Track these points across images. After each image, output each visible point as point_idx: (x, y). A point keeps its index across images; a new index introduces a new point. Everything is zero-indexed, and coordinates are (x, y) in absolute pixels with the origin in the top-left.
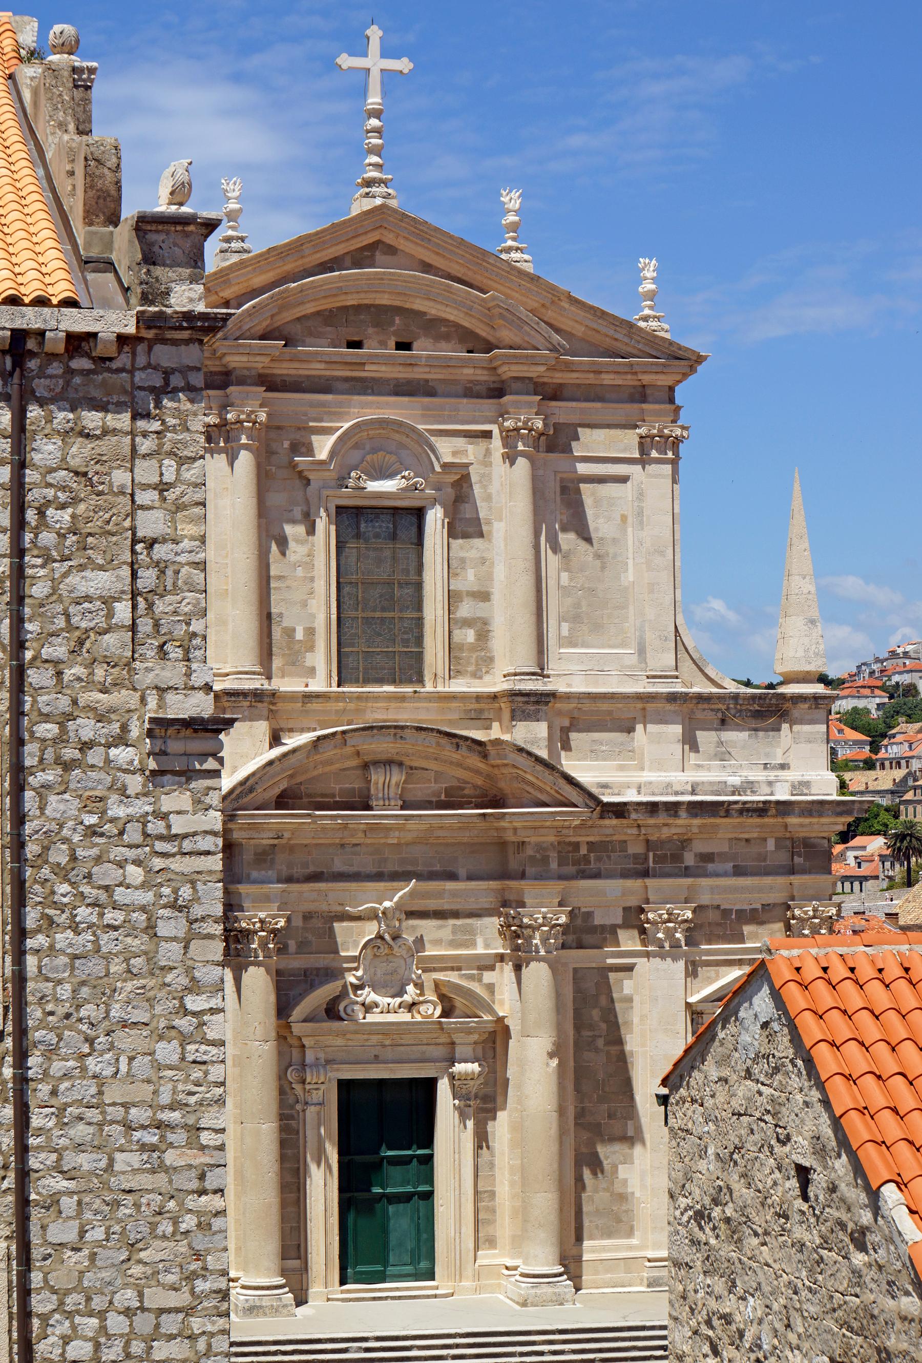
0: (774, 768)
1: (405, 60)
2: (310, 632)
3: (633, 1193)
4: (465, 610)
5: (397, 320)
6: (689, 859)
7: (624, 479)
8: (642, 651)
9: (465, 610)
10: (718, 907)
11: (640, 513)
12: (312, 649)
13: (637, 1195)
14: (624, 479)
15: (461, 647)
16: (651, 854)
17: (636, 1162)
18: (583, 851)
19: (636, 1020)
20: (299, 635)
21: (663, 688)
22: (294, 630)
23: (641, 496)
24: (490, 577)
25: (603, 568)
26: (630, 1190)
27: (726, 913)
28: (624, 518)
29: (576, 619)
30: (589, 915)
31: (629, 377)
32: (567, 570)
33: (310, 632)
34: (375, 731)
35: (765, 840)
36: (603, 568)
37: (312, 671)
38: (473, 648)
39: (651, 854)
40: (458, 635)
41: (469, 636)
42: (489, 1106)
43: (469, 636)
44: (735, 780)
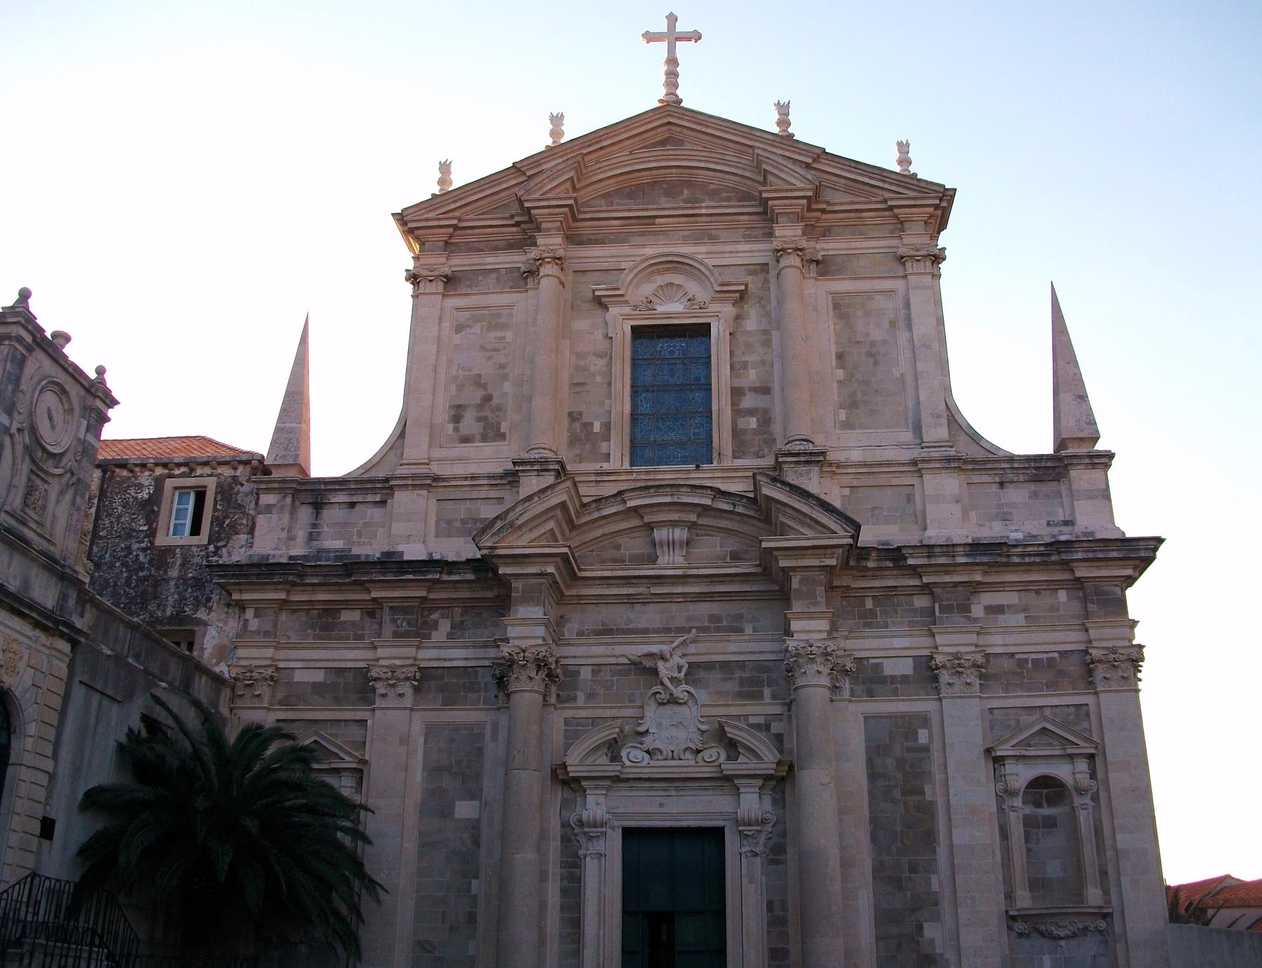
0: (1057, 525)
2: (607, 426)
4: (748, 401)
5: (685, 192)
6: (977, 611)
9: (748, 401)
10: (1012, 655)
16: (937, 605)
18: (869, 604)
20: (597, 427)
22: (592, 424)
23: (907, 305)
24: (770, 374)
25: (876, 363)
27: (1022, 663)
30: (878, 667)
32: (843, 368)
33: (607, 426)
36: (876, 363)
37: (607, 457)
38: (755, 432)
39: (937, 605)
41: (753, 423)
42: (780, 858)
43: (753, 423)
44: (1019, 536)
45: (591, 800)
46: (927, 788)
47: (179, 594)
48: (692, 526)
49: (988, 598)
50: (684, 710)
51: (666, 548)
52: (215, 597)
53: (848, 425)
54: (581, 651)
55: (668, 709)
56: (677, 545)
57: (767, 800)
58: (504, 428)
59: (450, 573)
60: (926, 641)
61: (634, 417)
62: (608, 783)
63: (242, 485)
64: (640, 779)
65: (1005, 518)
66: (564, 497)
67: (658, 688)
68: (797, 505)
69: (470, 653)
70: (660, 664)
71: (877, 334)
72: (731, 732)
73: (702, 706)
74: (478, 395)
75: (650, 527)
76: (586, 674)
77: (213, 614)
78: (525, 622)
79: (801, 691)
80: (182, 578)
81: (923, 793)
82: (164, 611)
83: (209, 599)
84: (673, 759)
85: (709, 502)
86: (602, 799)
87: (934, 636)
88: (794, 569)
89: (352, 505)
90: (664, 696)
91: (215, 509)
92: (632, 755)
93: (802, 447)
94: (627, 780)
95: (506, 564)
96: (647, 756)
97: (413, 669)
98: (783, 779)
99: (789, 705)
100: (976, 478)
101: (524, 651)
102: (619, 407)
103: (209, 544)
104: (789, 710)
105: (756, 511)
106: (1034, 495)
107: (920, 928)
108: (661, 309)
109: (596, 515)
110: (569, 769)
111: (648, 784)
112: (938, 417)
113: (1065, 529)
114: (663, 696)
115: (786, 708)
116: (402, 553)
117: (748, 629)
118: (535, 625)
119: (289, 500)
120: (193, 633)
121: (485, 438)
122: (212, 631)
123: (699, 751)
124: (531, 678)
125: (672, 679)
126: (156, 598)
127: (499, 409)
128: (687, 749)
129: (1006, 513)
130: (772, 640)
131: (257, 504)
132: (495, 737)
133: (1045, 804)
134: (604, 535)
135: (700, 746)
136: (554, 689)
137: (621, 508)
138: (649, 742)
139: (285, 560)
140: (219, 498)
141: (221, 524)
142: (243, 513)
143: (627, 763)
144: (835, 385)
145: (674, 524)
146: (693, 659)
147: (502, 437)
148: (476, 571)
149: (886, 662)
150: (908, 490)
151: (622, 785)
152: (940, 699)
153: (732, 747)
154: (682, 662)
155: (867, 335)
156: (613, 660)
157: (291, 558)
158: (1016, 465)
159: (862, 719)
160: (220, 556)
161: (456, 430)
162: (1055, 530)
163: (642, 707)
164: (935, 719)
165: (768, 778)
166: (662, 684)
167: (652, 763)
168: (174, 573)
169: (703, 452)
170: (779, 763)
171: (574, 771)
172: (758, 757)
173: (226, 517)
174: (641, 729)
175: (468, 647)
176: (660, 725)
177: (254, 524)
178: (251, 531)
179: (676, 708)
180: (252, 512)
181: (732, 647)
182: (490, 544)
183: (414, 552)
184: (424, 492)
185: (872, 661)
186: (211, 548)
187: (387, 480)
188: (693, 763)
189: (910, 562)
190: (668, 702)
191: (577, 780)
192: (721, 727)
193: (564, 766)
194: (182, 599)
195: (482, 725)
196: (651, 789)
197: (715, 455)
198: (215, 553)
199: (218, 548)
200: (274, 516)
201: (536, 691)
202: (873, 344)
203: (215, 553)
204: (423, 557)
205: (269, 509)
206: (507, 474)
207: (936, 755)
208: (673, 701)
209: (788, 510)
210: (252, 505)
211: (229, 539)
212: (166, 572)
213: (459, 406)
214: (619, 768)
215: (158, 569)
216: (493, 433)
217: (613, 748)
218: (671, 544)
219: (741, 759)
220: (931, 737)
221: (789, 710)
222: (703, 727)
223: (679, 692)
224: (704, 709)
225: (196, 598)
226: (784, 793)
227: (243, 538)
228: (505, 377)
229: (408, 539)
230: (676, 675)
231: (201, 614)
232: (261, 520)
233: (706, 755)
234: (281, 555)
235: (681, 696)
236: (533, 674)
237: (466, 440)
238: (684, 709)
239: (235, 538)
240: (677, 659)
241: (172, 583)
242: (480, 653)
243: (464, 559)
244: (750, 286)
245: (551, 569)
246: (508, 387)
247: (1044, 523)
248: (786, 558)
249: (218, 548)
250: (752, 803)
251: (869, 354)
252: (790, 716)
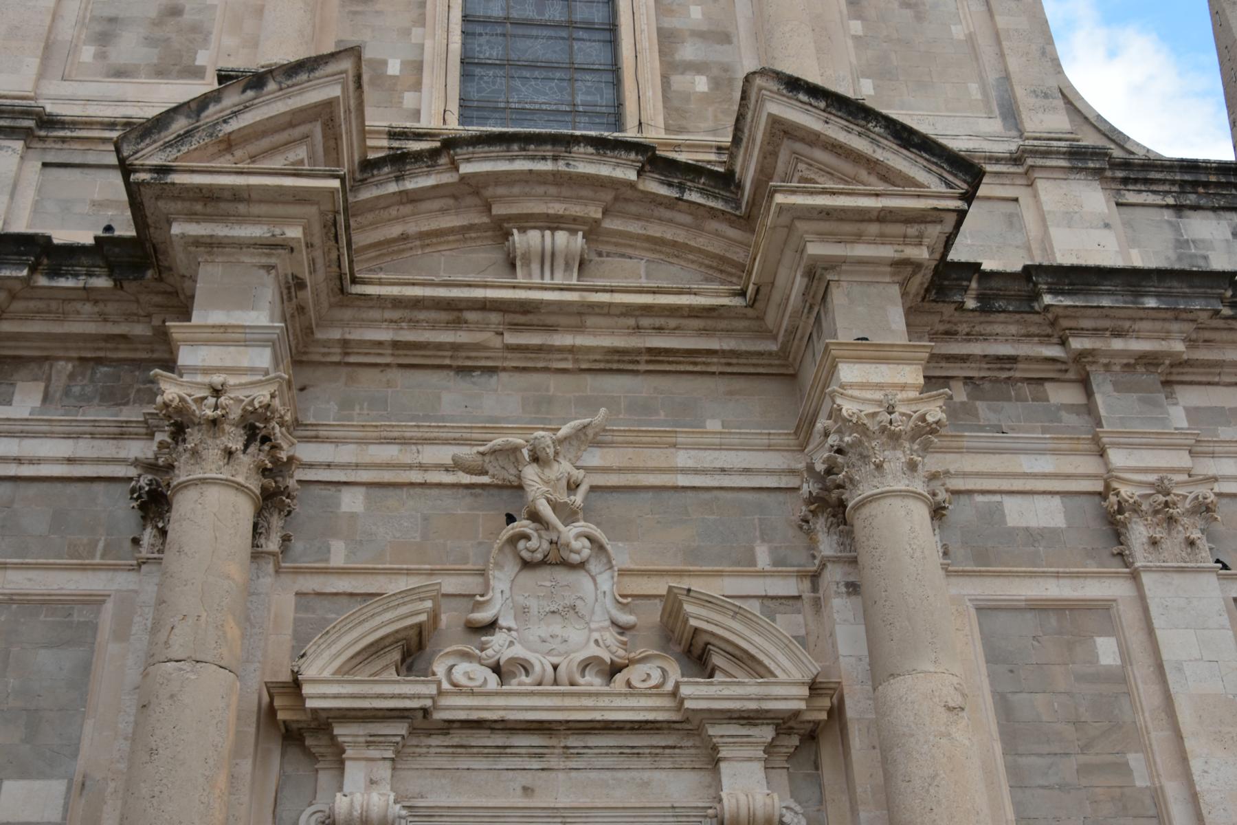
4: (688, 52)
9: (688, 52)
15: (687, 97)
20: (394, 68)
22: (384, 63)
32: (859, 17)
45: (355, 773)
46: (1135, 760)
48: (592, 231)
49: (1190, 397)
50: (582, 581)
51: (535, 267)
54: (346, 454)
55: (544, 577)
56: (560, 262)
57: (781, 777)
59: (54, 273)
60: (1089, 465)
61: (468, 63)
62: (401, 728)
64: (478, 724)
66: (335, 91)
67: (523, 525)
68: (842, 137)
69: (83, 448)
70: (531, 473)
72: (697, 616)
73: (623, 573)
75: (501, 230)
78: (223, 335)
79: (865, 511)
81: (1123, 768)
84: (556, 682)
85: (632, 175)
86: (384, 771)
87: (1102, 453)
88: (833, 264)
90: (537, 545)
92: (459, 680)
94: (449, 726)
95: (192, 217)
96: (493, 679)
98: (812, 736)
99: (815, 577)
100: (1131, 197)
101: (217, 392)
102: (440, 33)
104: (815, 588)
105: (726, 200)
109: (393, 188)
110: (307, 690)
111: (499, 739)
114: (534, 543)
115: (807, 584)
117: (713, 425)
118: (246, 343)
123: (613, 670)
124: (229, 454)
125: (555, 506)
127: (195, 28)
128: (585, 665)
130: (769, 448)
132: (122, 634)
134: (404, 237)
135: (621, 654)
136: (276, 521)
137: (448, 178)
138: (499, 646)
143: (446, 686)
144: (850, 43)
145: (553, 223)
146: (600, 480)
148: (112, 269)
149: (1010, 503)
150: (1010, 207)
151: (435, 741)
152: (1135, 576)
153: (697, 655)
154: (578, 475)
156: (416, 476)
158: (1203, 178)
159: (973, 612)
163: (482, 573)
164: (1128, 615)
165: (784, 723)
166: (535, 517)
170: (815, 688)
171: (322, 693)
174: (483, 616)
175: (77, 436)
176: (525, 610)
179: (563, 576)
181: (683, 459)
182: (156, 161)
184: (19, 145)
185: (979, 498)
189: (1048, 299)
190: (543, 563)
191: (323, 723)
192: (672, 605)
193: (295, 685)
195: (94, 601)
196: (502, 751)
201: (239, 487)
207: (1147, 694)
208: (557, 560)
209: (820, 155)
213: (112, 20)
214: (433, 690)
217: (412, 650)
218: (548, 259)
219: (719, 677)
220: (1124, 653)
221: (815, 588)
222: (626, 618)
223: (571, 534)
224: (626, 580)
226: (817, 768)
230: (563, 497)
233: (635, 674)
235: (576, 545)
236: (237, 444)
237: (120, 73)
238: (582, 579)
240: (563, 468)
242: (107, 449)
245: (294, 233)
248: (823, 237)
250: (747, 784)
252: (817, 604)
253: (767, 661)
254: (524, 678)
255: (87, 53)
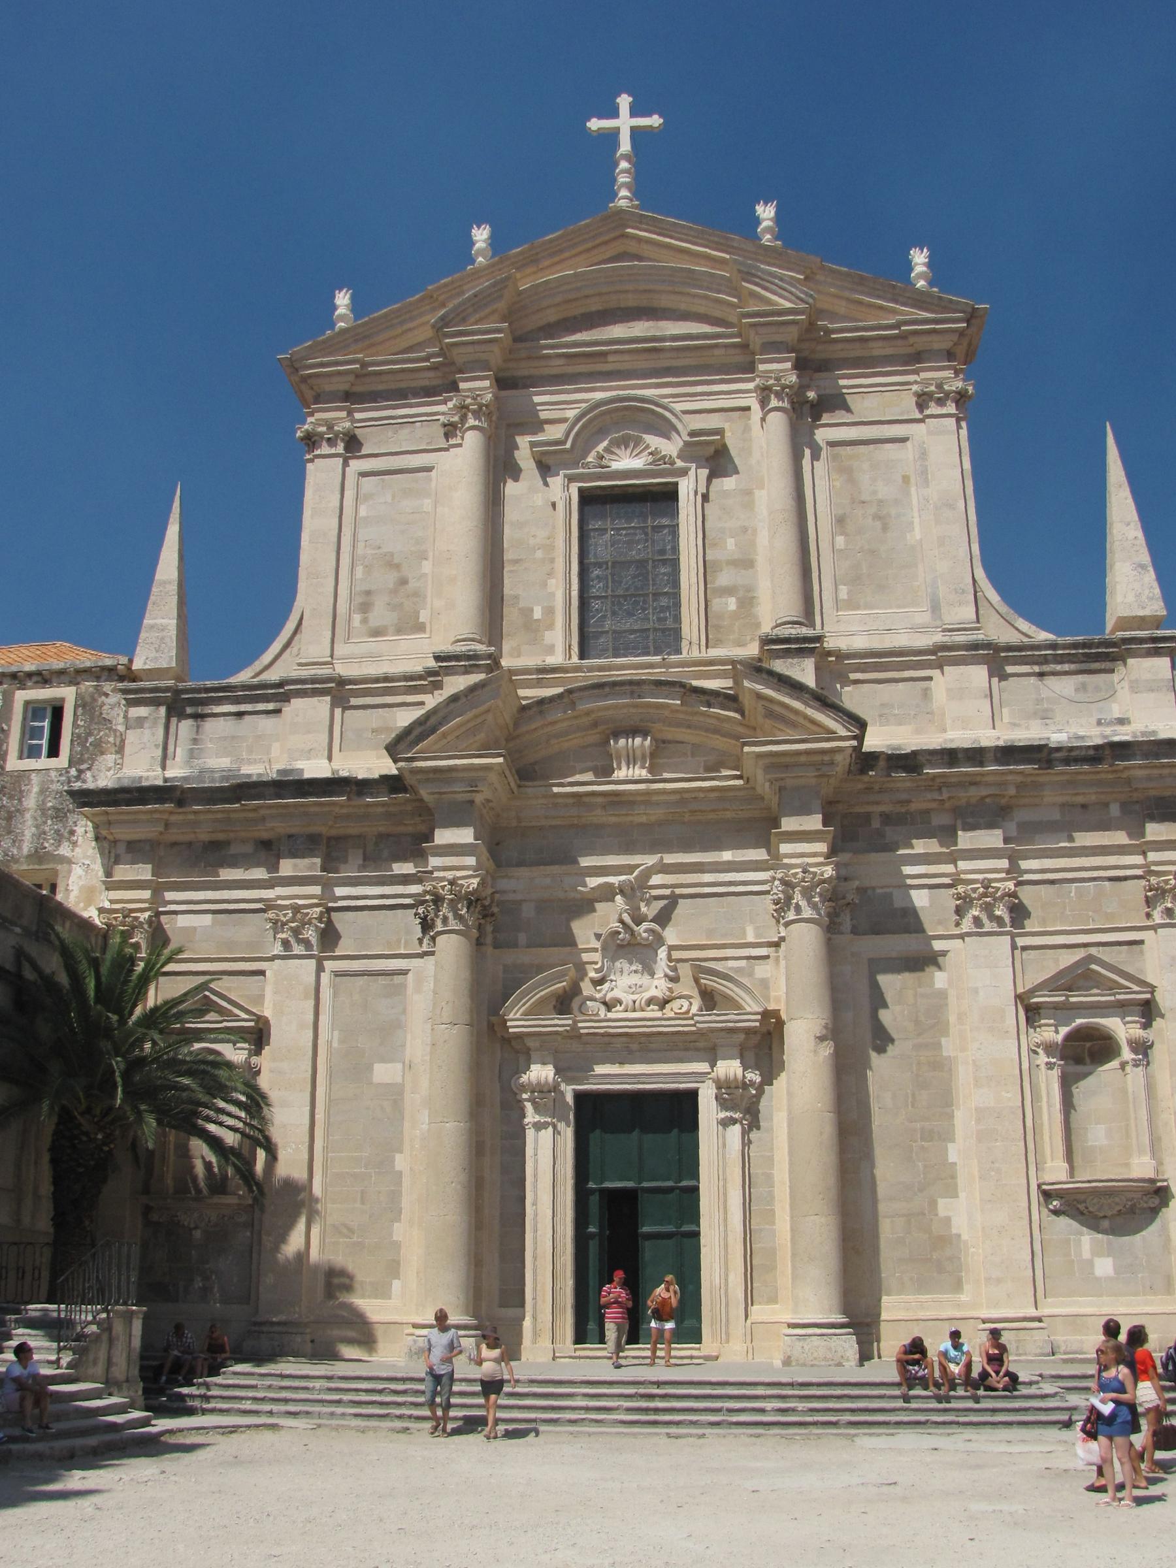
1: (656, 117)
3: (959, 1236)
4: (724, 579)
7: (904, 440)
8: (935, 608)
11: (924, 472)
12: (551, 626)
13: (965, 1237)
14: (904, 440)
17: (962, 1195)
18: (876, 824)
19: (952, 1019)
20: (538, 614)
21: (960, 638)
22: (532, 610)
23: (924, 454)
25: (885, 528)
26: (954, 1231)
28: (906, 479)
29: (855, 580)
31: (899, 342)
33: (549, 611)
34: (607, 690)
35: (1106, 805)
36: (885, 528)
38: (735, 616)
40: (716, 604)
43: (732, 604)
47: (37, 827)
52: (80, 830)
53: (852, 604)
58: (424, 616)
63: (107, 695)
65: (1045, 716)
71: (884, 491)
74: (391, 578)
76: (528, 911)
77: (77, 850)
80: (42, 809)
81: (938, 1046)
82: (20, 848)
83: (72, 833)
84: (634, 1010)
89: (240, 715)
91: (75, 725)
93: (793, 631)
97: (318, 910)
103: (70, 766)
106: (1083, 688)
107: (933, 1204)
108: (616, 465)
112: (963, 592)
113: (1119, 728)
116: (302, 770)
119: (163, 710)
120: (55, 873)
121: (399, 631)
122: (77, 871)
126: (9, 832)
129: (1046, 710)
131: (126, 717)
133: (1088, 1060)
139: (160, 782)
140: (80, 711)
141: (83, 744)
142: (110, 729)
147: (420, 628)
155: (875, 492)
157: (166, 780)
160: (84, 781)
161: (364, 621)
162: (1108, 731)
167: (610, 1015)
168: (31, 802)
169: (670, 639)
172: (738, 1006)
173: (90, 734)
177: (123, 741)
178: (120, 750)
180: (121, 728)
183: (316, 768)
186: (73, 772)
187: (280, 685)
188: (659, 1014)
194: (41, 835)
197: (684, 644)
198: (78, 778)
199: (80, 772)
200: (147, 732)
202: (880, 502)
203: (78, 778)
204: (328, 774)
205: (140, 722)
206: (431, 673)
210: (121, 719)
211: (93, 760)
212: (20, 800)
213: (368, 593)
215: (11, 798)
216: (413, 625)
225: (57, 832)
226: (770, 1048)
227: (110, 758)
228: (423, 556)
229: (309, 754)
231: (65, 850)
232: (131, 737)
234: (153, 776)
237: (377, 632)
239: (100, 759)
241: (28, 816)
243: (376, 776)
244: (728, 434)
246: (427, 567)
247: (1094, 721)
249: (80, 772)
251: (877, 517)
253: (741, 1001)
254: (621, 1009)
255: (357, 618)
